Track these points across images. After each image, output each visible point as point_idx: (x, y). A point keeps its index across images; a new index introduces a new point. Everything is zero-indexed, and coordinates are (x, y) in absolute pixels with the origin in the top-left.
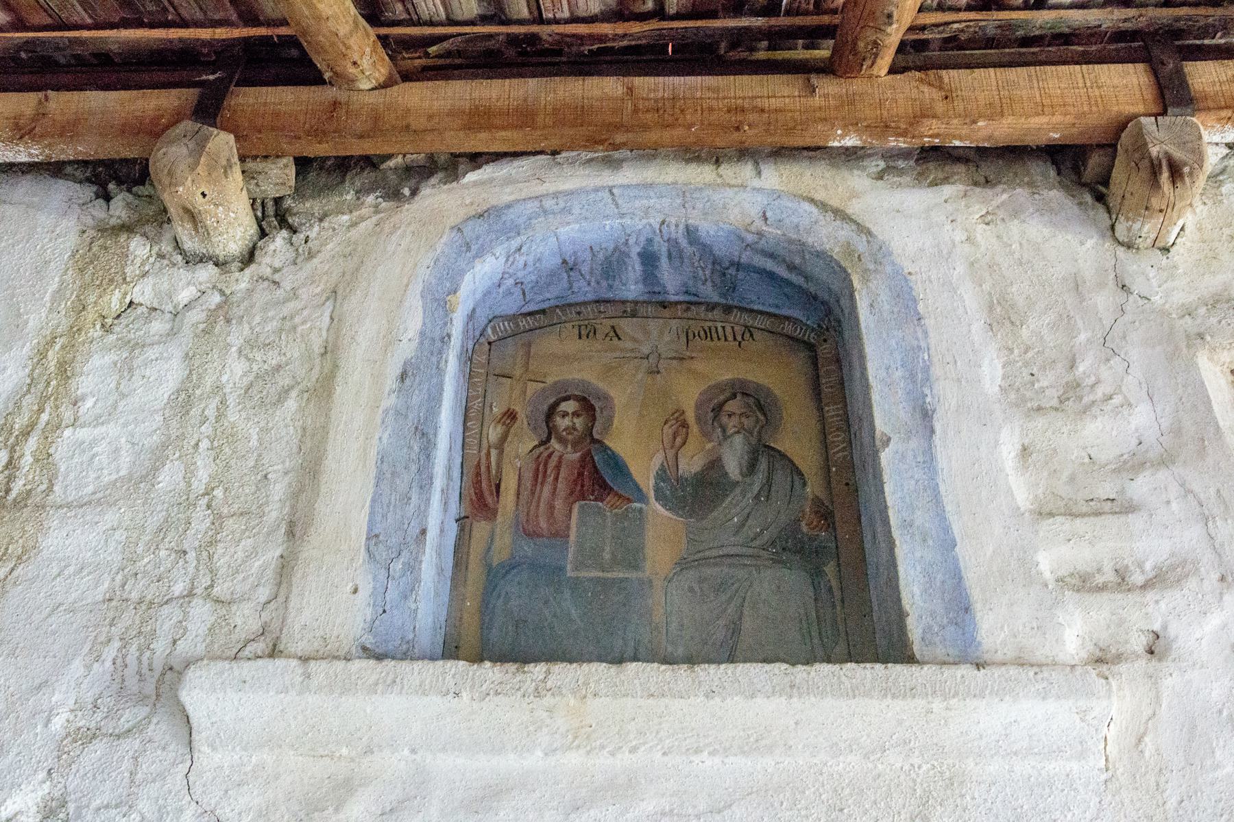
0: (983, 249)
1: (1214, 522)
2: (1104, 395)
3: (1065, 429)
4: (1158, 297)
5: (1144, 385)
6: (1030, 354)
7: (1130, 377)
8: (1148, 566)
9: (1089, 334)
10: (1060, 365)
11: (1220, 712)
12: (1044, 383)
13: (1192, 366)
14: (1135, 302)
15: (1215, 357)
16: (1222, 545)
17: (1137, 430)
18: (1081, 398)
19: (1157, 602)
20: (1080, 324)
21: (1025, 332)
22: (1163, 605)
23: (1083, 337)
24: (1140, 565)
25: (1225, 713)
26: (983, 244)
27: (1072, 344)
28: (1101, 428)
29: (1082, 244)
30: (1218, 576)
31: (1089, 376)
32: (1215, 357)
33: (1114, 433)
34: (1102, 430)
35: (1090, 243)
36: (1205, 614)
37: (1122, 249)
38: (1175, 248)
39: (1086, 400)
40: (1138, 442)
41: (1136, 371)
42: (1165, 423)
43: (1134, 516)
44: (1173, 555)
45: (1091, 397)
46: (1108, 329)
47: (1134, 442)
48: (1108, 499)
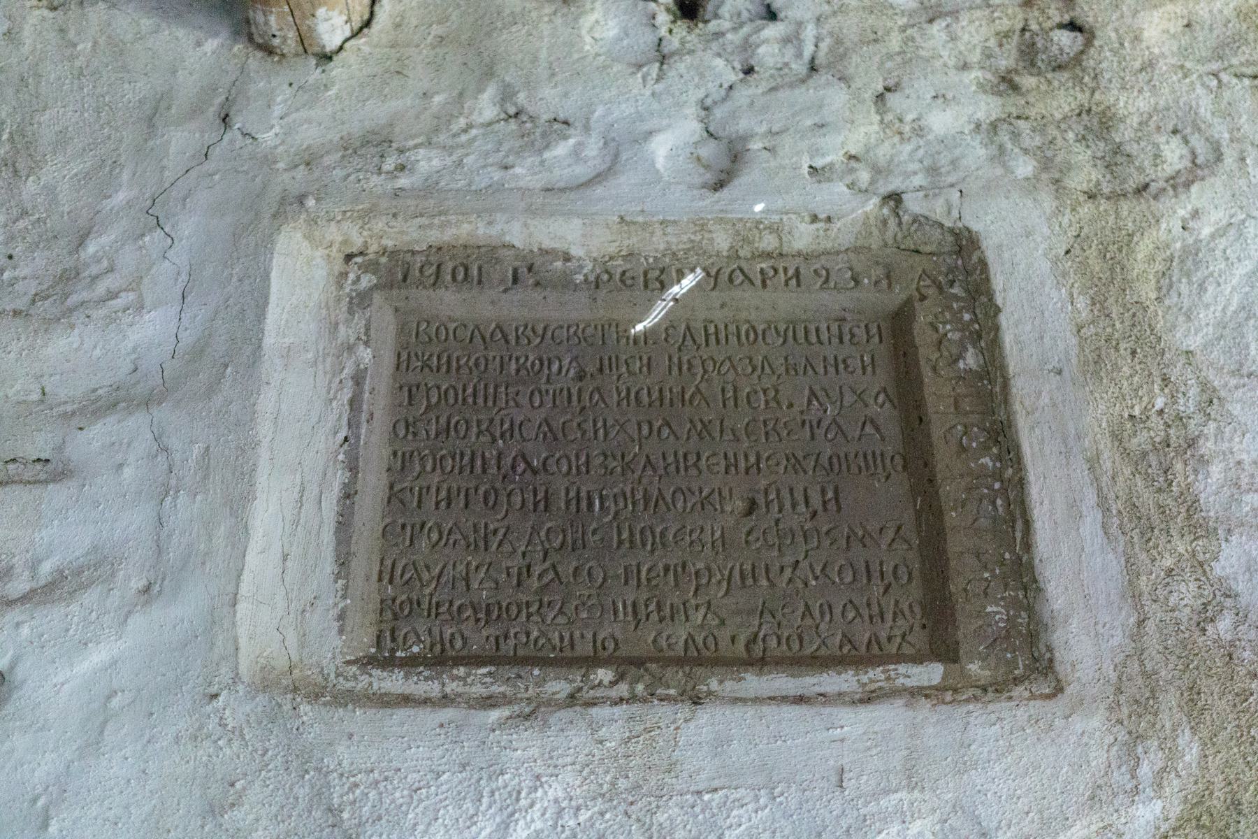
0: (26, 49)
1: (175, 499)
2: (109, 291)
3: (14, 347)
4: (271, 133)
5: (184, 277)
6: (21, 224)
7: (167, 263)
8: (46, 568)
9: (134, 192)
10: (62, 243)
11: (34, 801)
12: (23, 271)
13: (266, 245)
14: (232, 142)
15: (317, 233)
16: (169, 536)
17: (134, 349)
18: (67, 296)
19: (18, 625)
20: (125, 177)
21: (30, 187)
22: (25, 631)
23: (120, 197)
24: (34, 566)
25: (40, 803)
26: (28, 42)
27: (98, 208)
28: (75, 346)
29: (199, 44)
30: (142, 583)
31: (99, 261)
32: (317, 233)
33: (97, 352)
34: (77, 350)
35: (211, 45)
36: (86, 644)
37: (259, 54)
38: (343, 54)
39: (74, 299)
40: (133, 367)
41: (179, 256)
42: (187, 338)
43: (58, 486)
44: (95, 548)
45: (85, 295)
46: (167, 185)
47: (127, 367)
48: (39, 460)
